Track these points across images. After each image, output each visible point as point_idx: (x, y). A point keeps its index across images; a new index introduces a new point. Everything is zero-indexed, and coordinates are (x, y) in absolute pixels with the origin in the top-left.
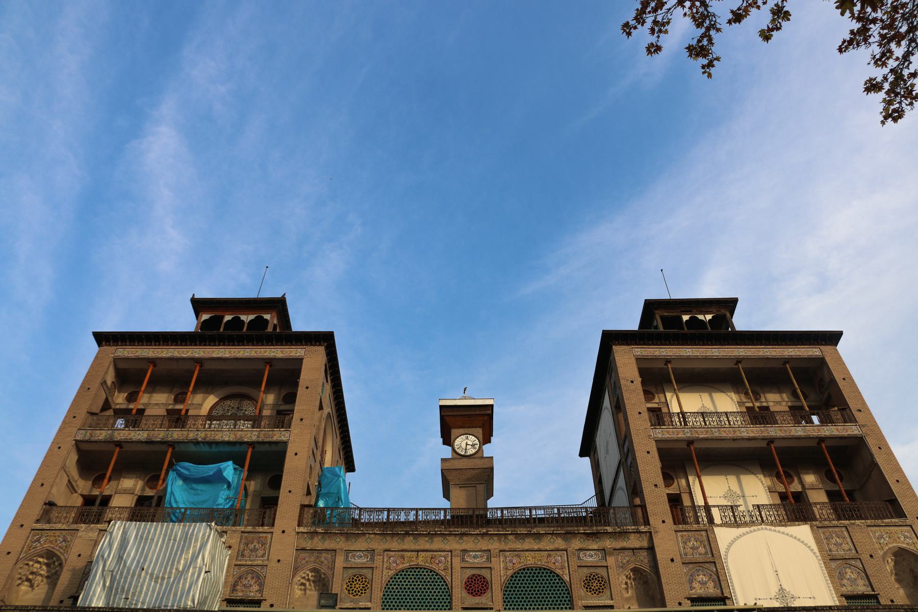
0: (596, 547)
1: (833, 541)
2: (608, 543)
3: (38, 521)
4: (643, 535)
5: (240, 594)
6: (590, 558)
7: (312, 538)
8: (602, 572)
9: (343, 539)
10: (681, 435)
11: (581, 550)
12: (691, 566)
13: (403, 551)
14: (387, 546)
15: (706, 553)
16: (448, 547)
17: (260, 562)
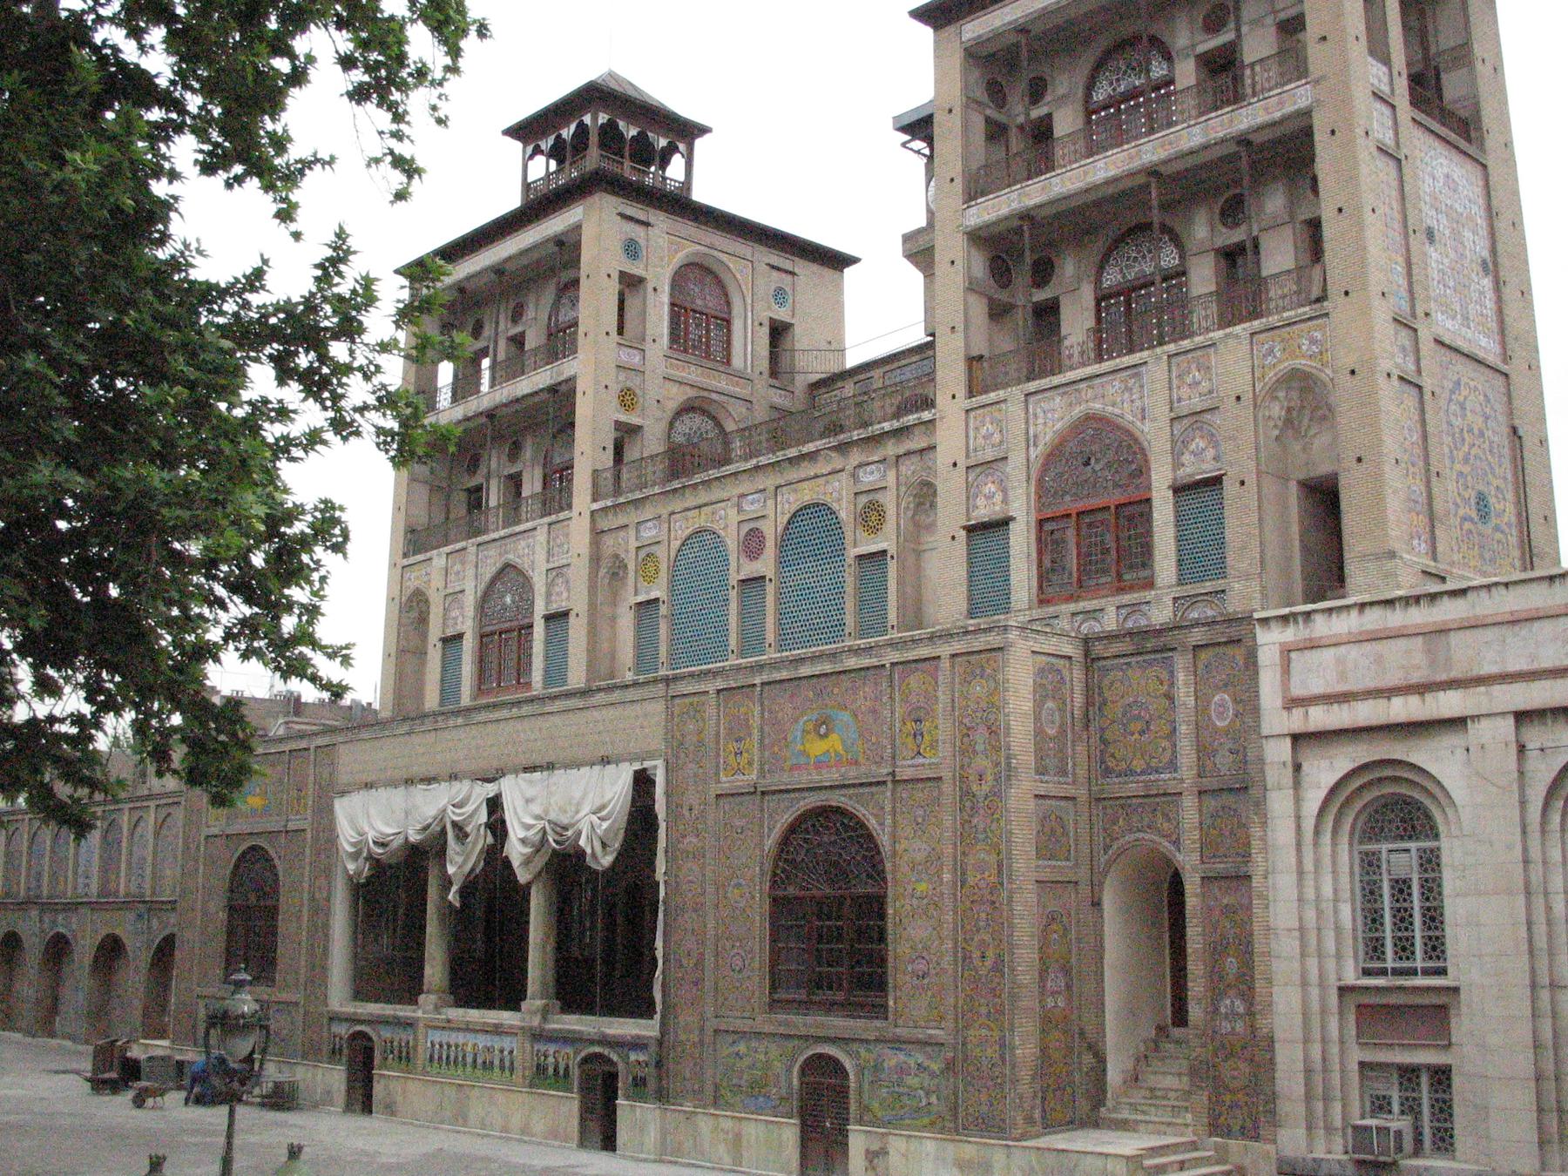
0: (876, 458)
1: (1189, 380)
2: (891, 449)
3: (405, 555)
4: (930, 426)
5: (555, 606)
6: (869, 478)
7: (606, 515)
8: (879, 496)
9: (631, 509)
10: (1004, 211)
11: (860, 466)
12: (978, 470)
13: (688, 509)
14: (670, 509)
15: (1001, 442)
16: (725, 495)
17: (565, 562)
